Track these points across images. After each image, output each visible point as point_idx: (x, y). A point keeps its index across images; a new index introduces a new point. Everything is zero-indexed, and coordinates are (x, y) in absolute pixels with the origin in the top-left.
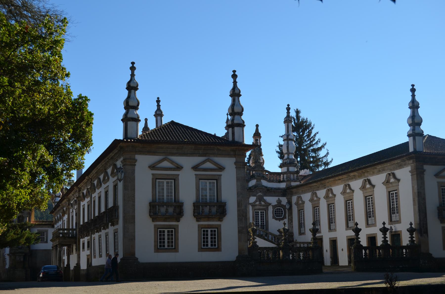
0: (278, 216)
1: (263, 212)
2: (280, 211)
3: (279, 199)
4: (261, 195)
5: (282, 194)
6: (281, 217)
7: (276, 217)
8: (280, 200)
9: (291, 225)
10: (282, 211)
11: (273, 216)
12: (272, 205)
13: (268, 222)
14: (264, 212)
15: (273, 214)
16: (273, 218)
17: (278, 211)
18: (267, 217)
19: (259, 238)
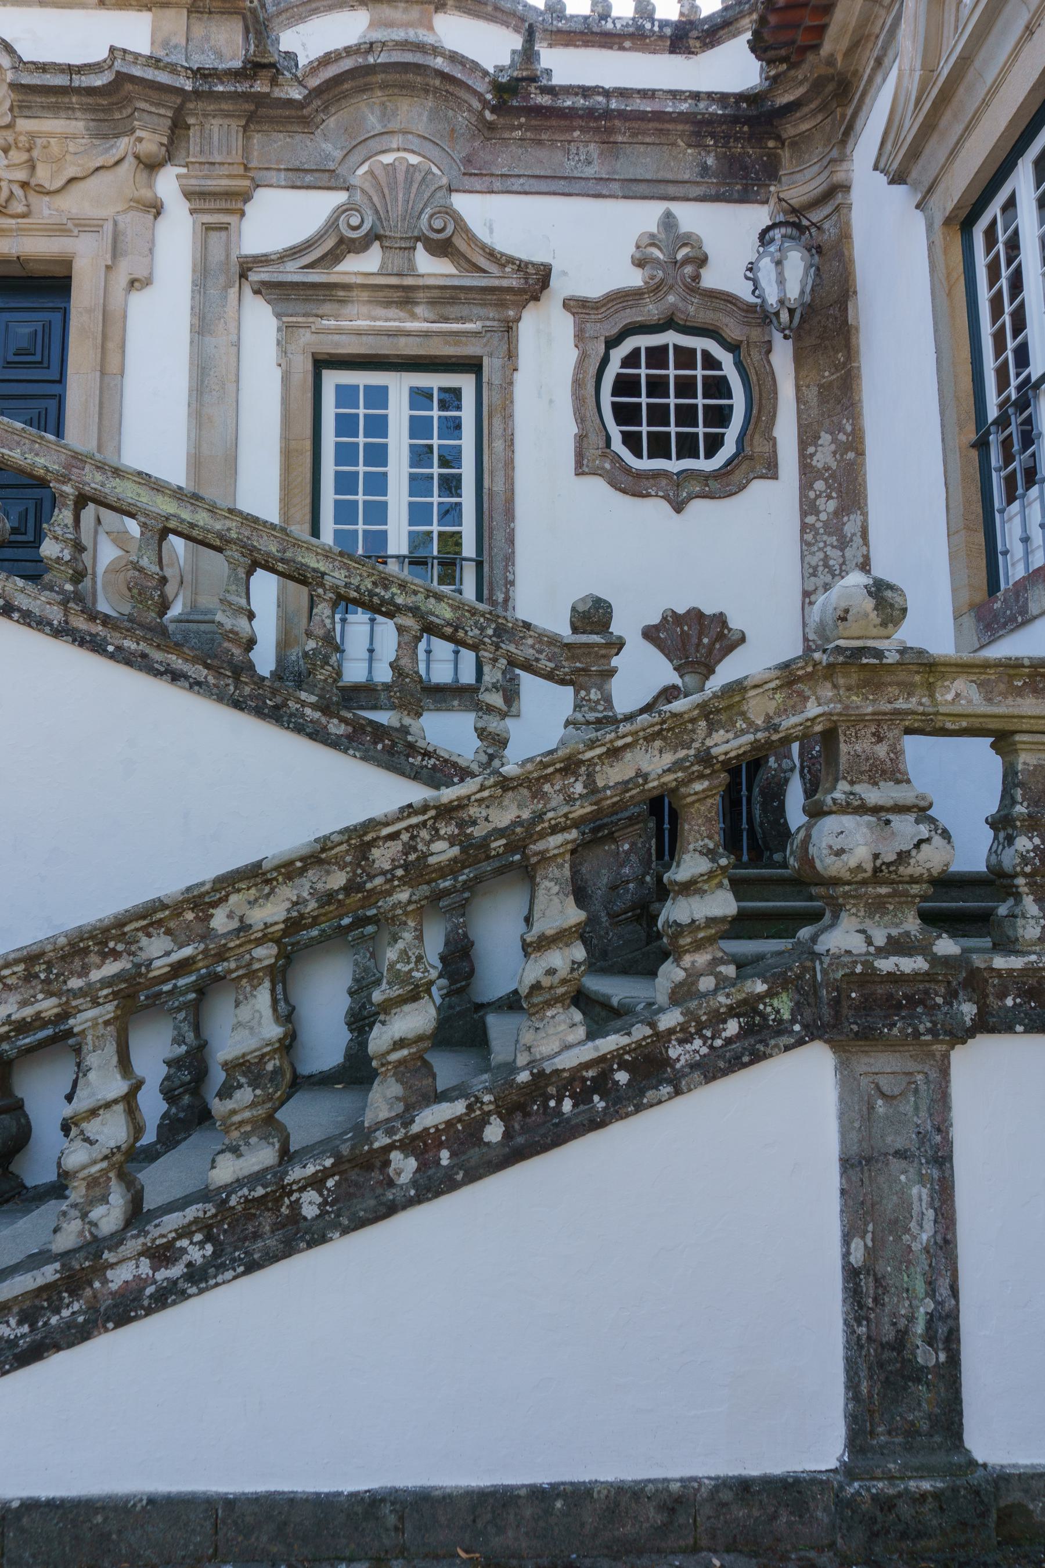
0: (659, 447)
1: (451, 398)
2: (686, 387)
3: (668, 221)
4: (411, 168)
5: (710, 161)
6: (709, 455)
7: (639, 455)
8: (688, 240)
9: (843, 544)
10: (724, 379)
11: (581, 439)
12: (561, 287)
13: (509, 514)
14: (456, 393)
15: (580, 419)
16: (581, 469)
17: (657, 387)
18: (499, 445)
19: (127, 659)
